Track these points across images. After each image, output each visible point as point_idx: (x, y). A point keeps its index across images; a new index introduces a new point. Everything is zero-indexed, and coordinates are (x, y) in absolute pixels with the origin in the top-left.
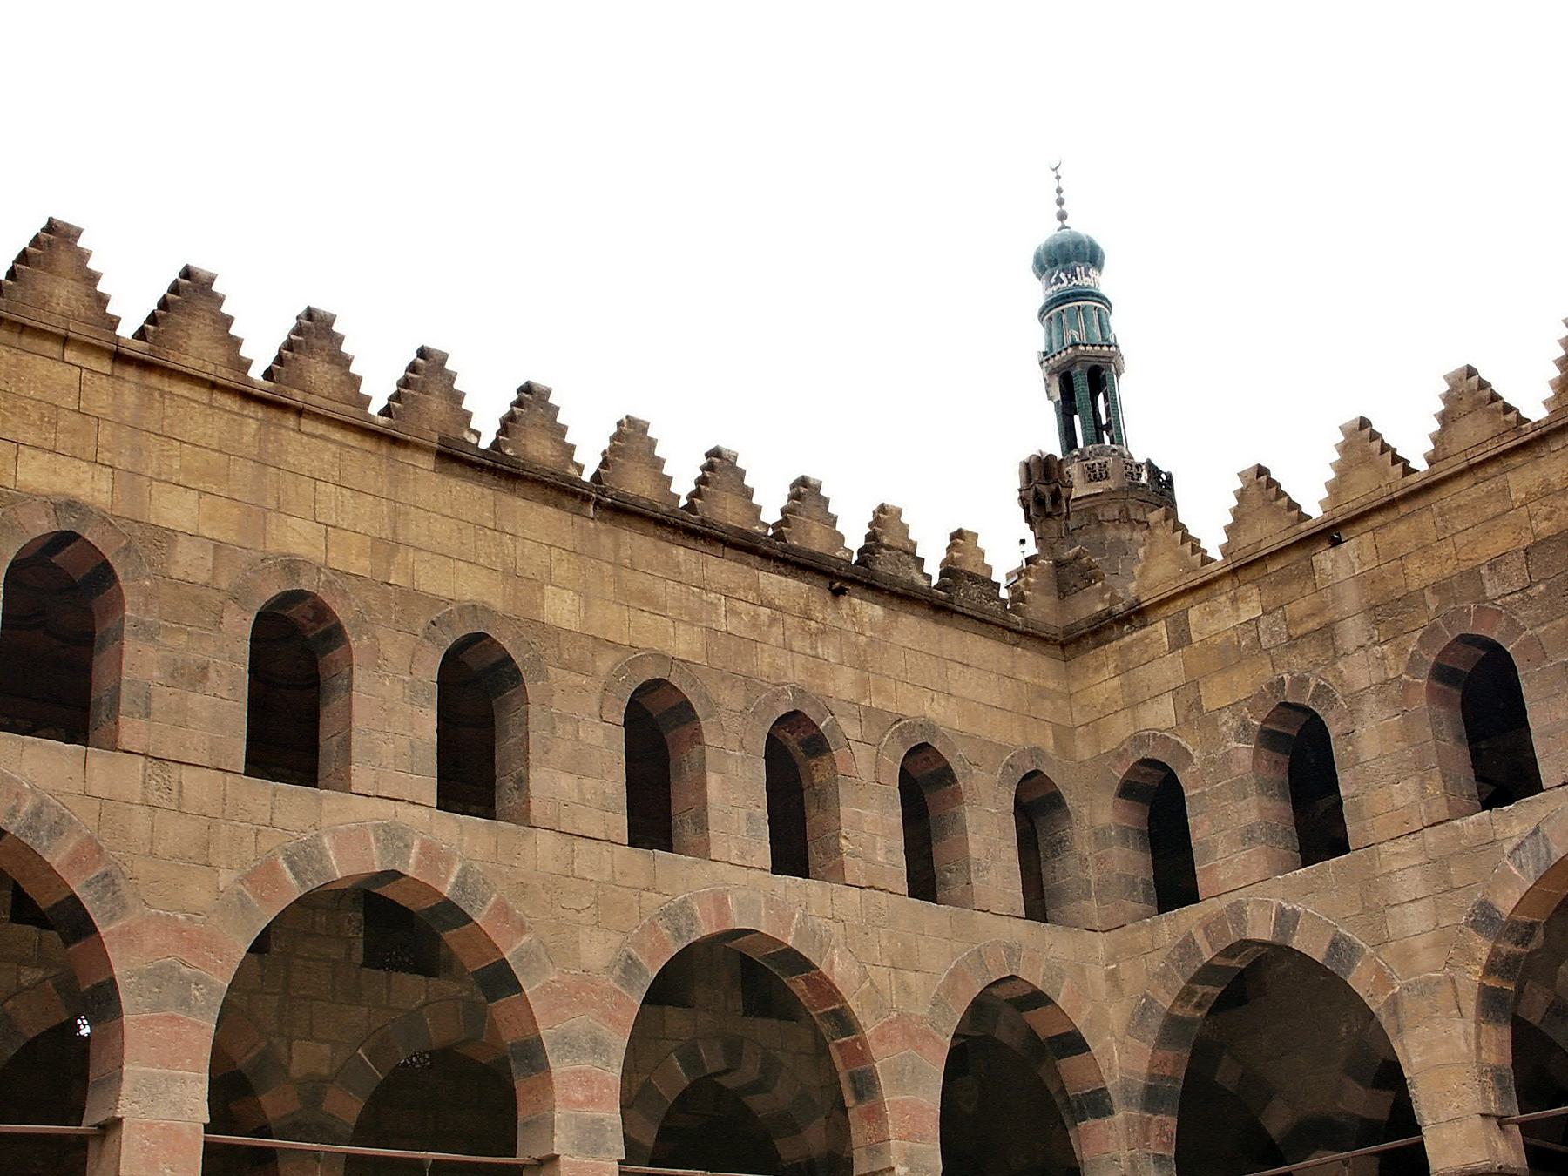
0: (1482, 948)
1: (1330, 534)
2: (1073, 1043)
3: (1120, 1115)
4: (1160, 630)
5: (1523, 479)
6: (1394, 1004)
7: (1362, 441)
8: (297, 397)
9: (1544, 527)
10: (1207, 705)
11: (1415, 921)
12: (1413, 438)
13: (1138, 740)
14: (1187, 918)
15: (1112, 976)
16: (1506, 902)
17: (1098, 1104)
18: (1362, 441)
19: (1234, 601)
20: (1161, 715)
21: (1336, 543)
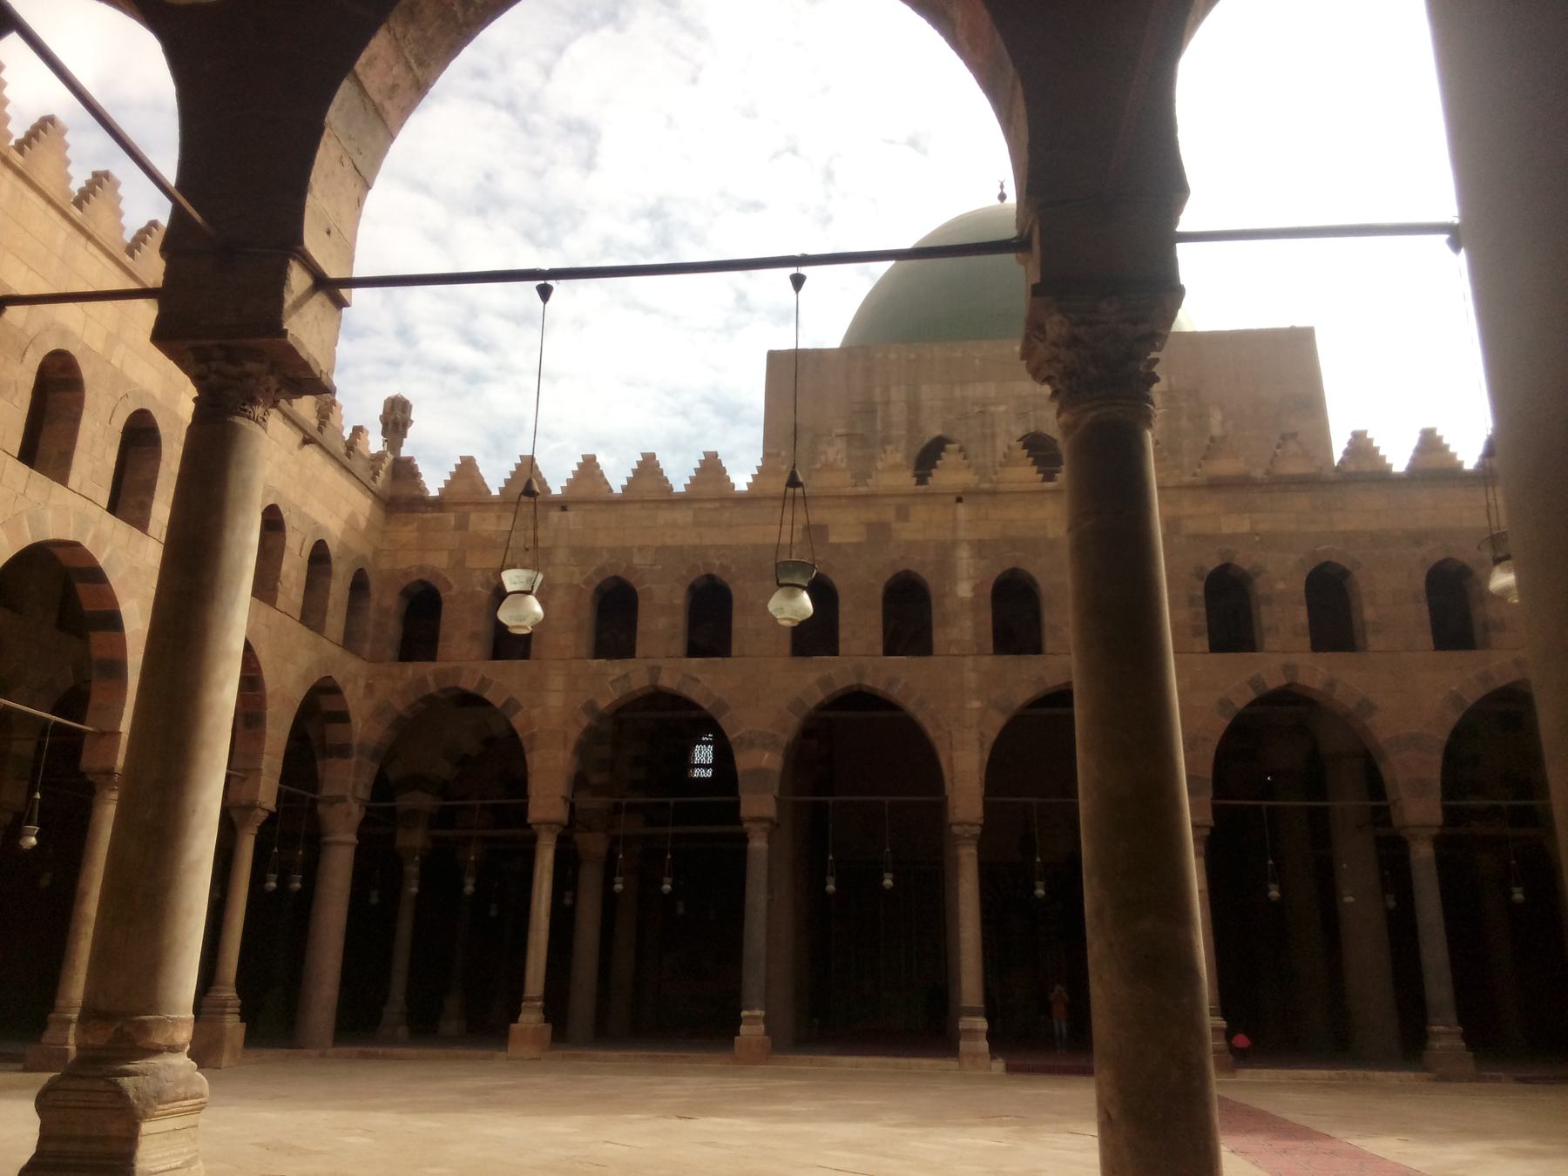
0: (585, 721)
1: (562, 504)
2: (343, 717)
3: (354, 759)
4: (451, 518)
5: (664, 516)
6: (533, 736)
7: (589, 467)
8: (90, 227)
9: (669, 541)
10: (469, 564)
11: (555, 701)
12: (617, 476)
13: (421, 569)
14: (426, 669)
15: (370, 688)
16: (603, 704)
17: (343, 751)
18: (589, 467)
19: (499, 517)
20: (438, 561)
21: (564, 509)
